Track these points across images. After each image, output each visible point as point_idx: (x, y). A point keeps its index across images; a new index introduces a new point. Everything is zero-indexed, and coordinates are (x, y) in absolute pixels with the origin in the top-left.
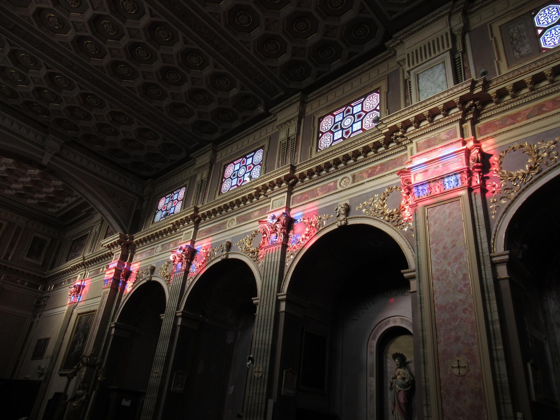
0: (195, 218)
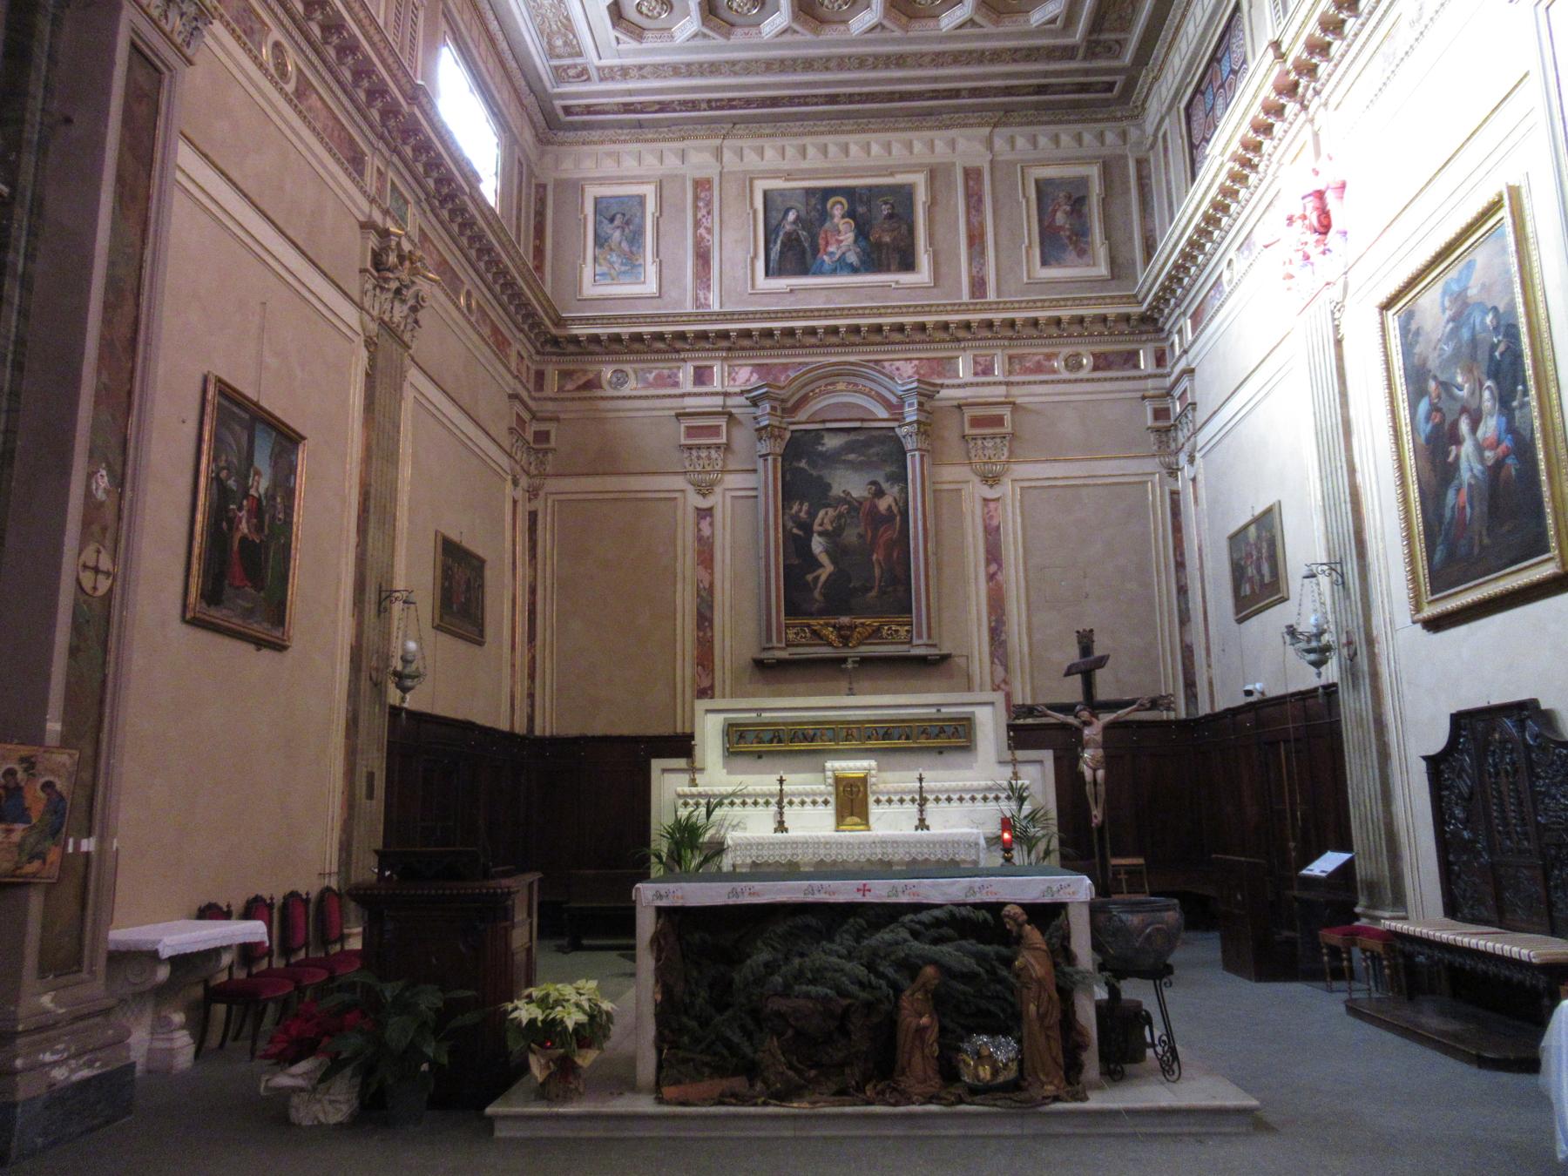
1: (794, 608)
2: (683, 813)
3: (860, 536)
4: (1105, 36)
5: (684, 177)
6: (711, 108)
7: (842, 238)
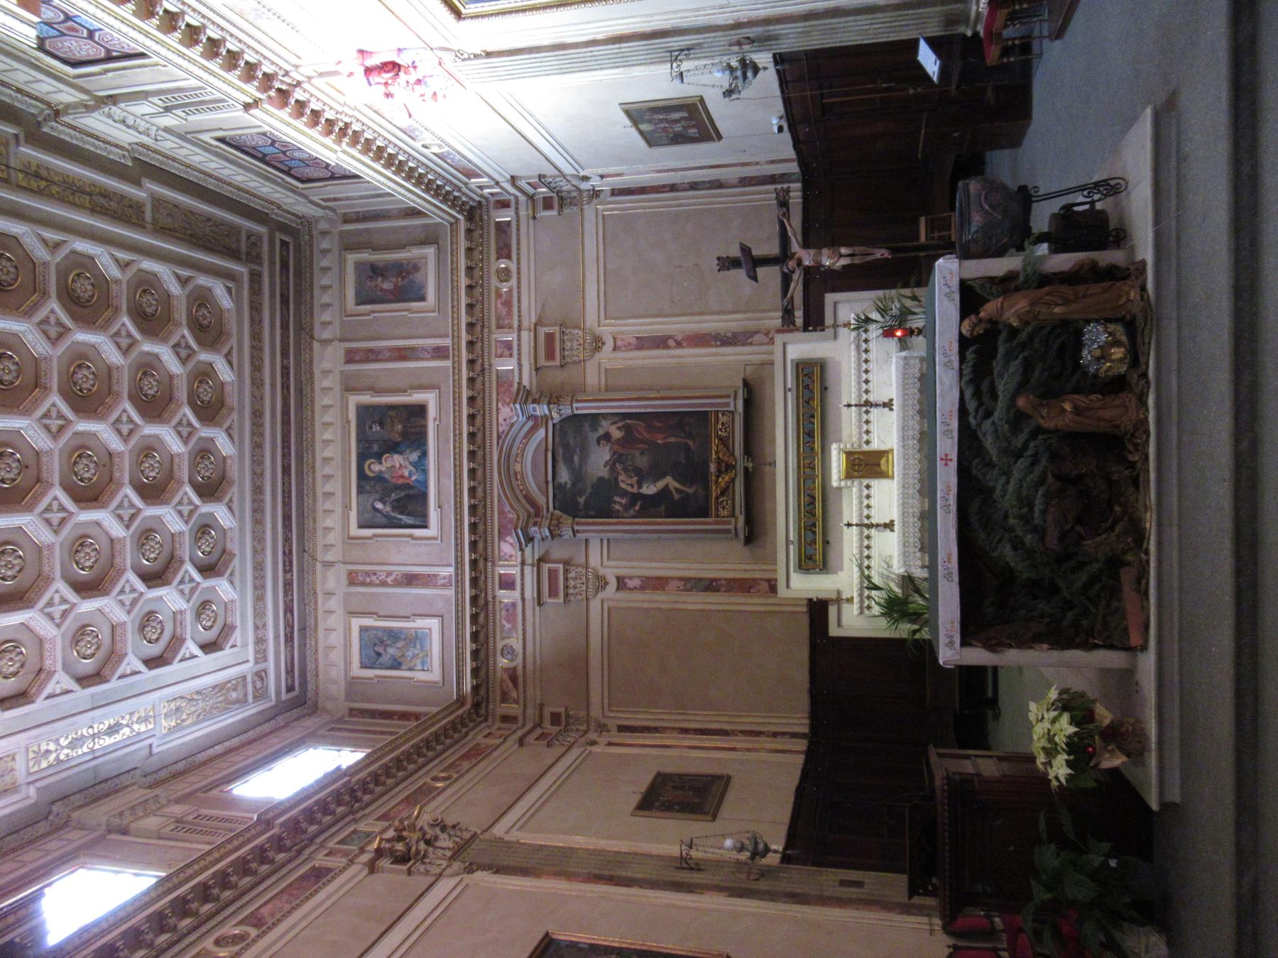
1: (703, 511)
2: (877, 610)
3: (642, 454)
4: (244, 249)
5: (347, 594)
6: (291, 570)
7: (397, 464)
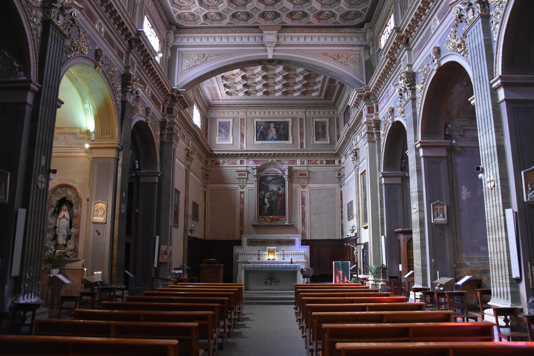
0: (402, 39)
7: (273, 132)
